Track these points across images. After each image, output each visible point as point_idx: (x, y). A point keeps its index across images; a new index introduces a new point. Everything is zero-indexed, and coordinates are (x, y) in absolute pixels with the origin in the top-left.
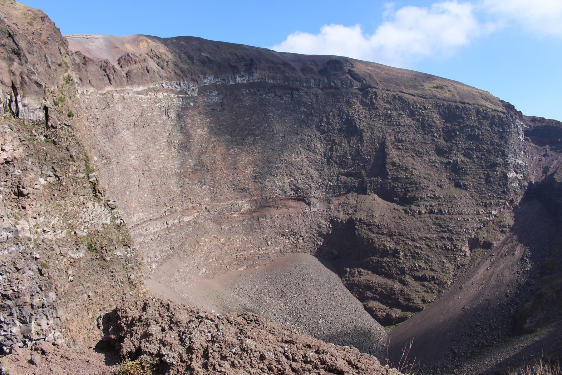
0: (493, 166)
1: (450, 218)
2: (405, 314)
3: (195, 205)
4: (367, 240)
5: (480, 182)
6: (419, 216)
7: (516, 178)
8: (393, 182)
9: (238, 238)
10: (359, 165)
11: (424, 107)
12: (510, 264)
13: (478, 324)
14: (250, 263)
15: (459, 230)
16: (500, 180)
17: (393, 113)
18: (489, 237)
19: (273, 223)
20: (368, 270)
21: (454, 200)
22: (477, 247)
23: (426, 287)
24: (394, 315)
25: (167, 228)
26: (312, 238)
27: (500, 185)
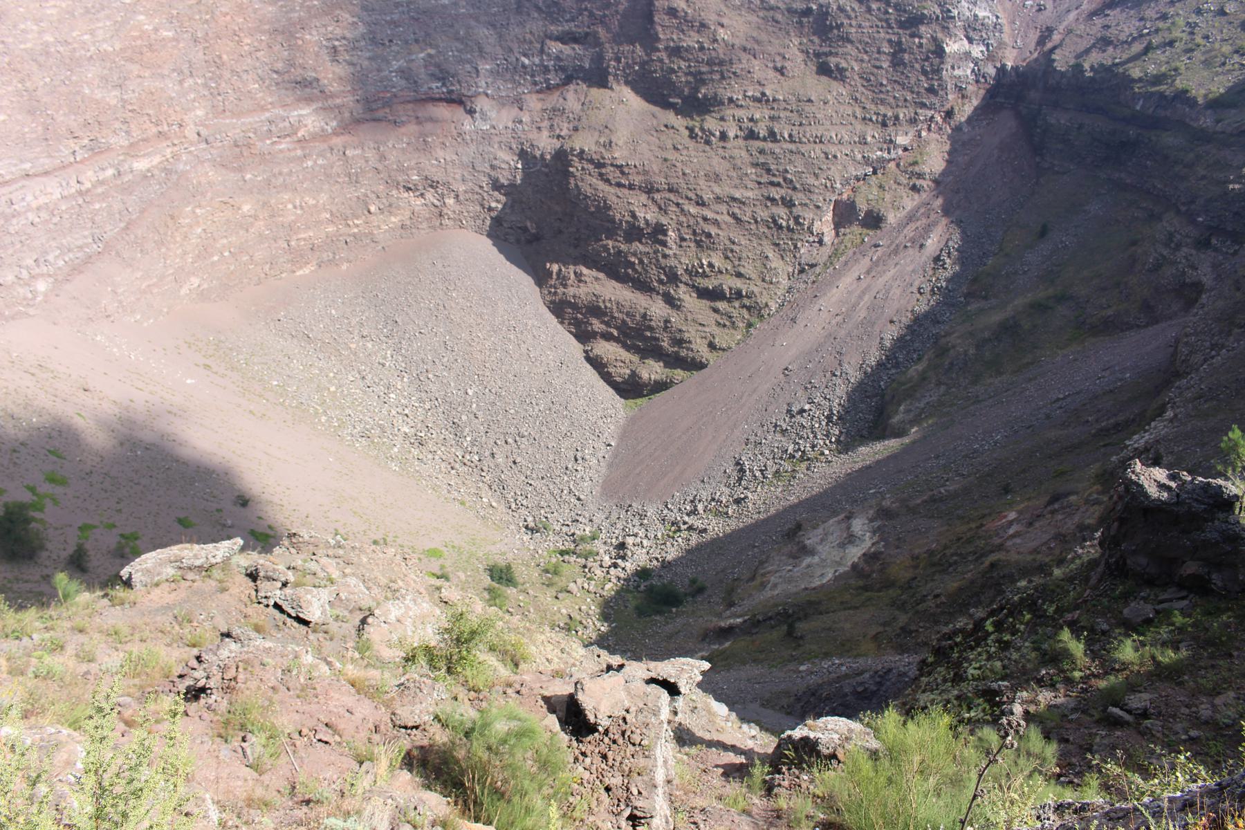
0: (913, 22)
2: (671, 374)
3: (166, 128)
4: (595, 200)
5: (878, 64)
6: (721, 144)
7: (967, 55)
8: (669, 56)
9: (290, 201)
10: (591, 15)
12: (909, 269)
13: (807, 407)
14: (325, 256)
15: (811, 180)
16: (927, 59)
18: (881, 201)
19: (380, 161)
20: (599, 270)
21: (808, 108)
22: (851, 223)
23: (722, 314)
24: (647, 376)
25: (80, 193)
26: (477, 193)
27: (925, 73)
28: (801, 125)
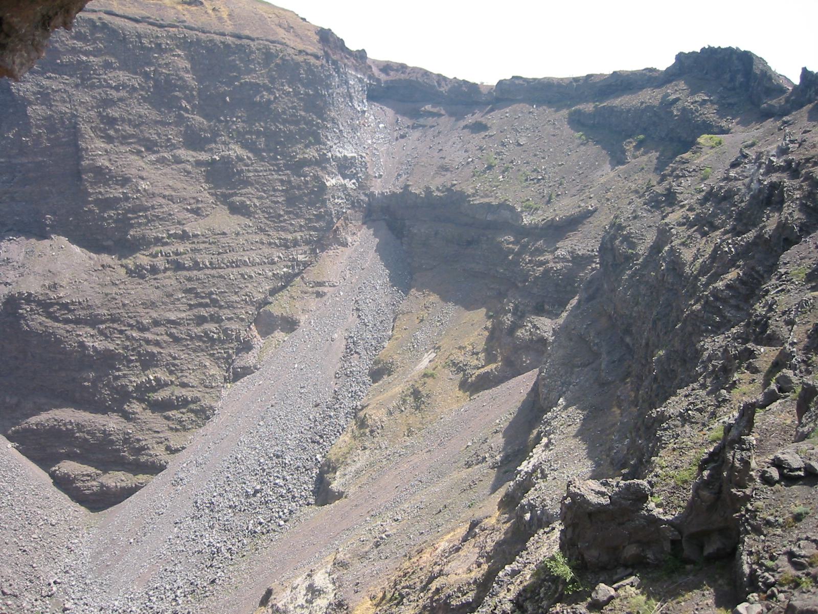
1: (213, 277)
11: (159, 45)
13: (258, 487)
15: (235, 298)
17: (92, 58)
23: (173, 420)
28: (219, 254)
